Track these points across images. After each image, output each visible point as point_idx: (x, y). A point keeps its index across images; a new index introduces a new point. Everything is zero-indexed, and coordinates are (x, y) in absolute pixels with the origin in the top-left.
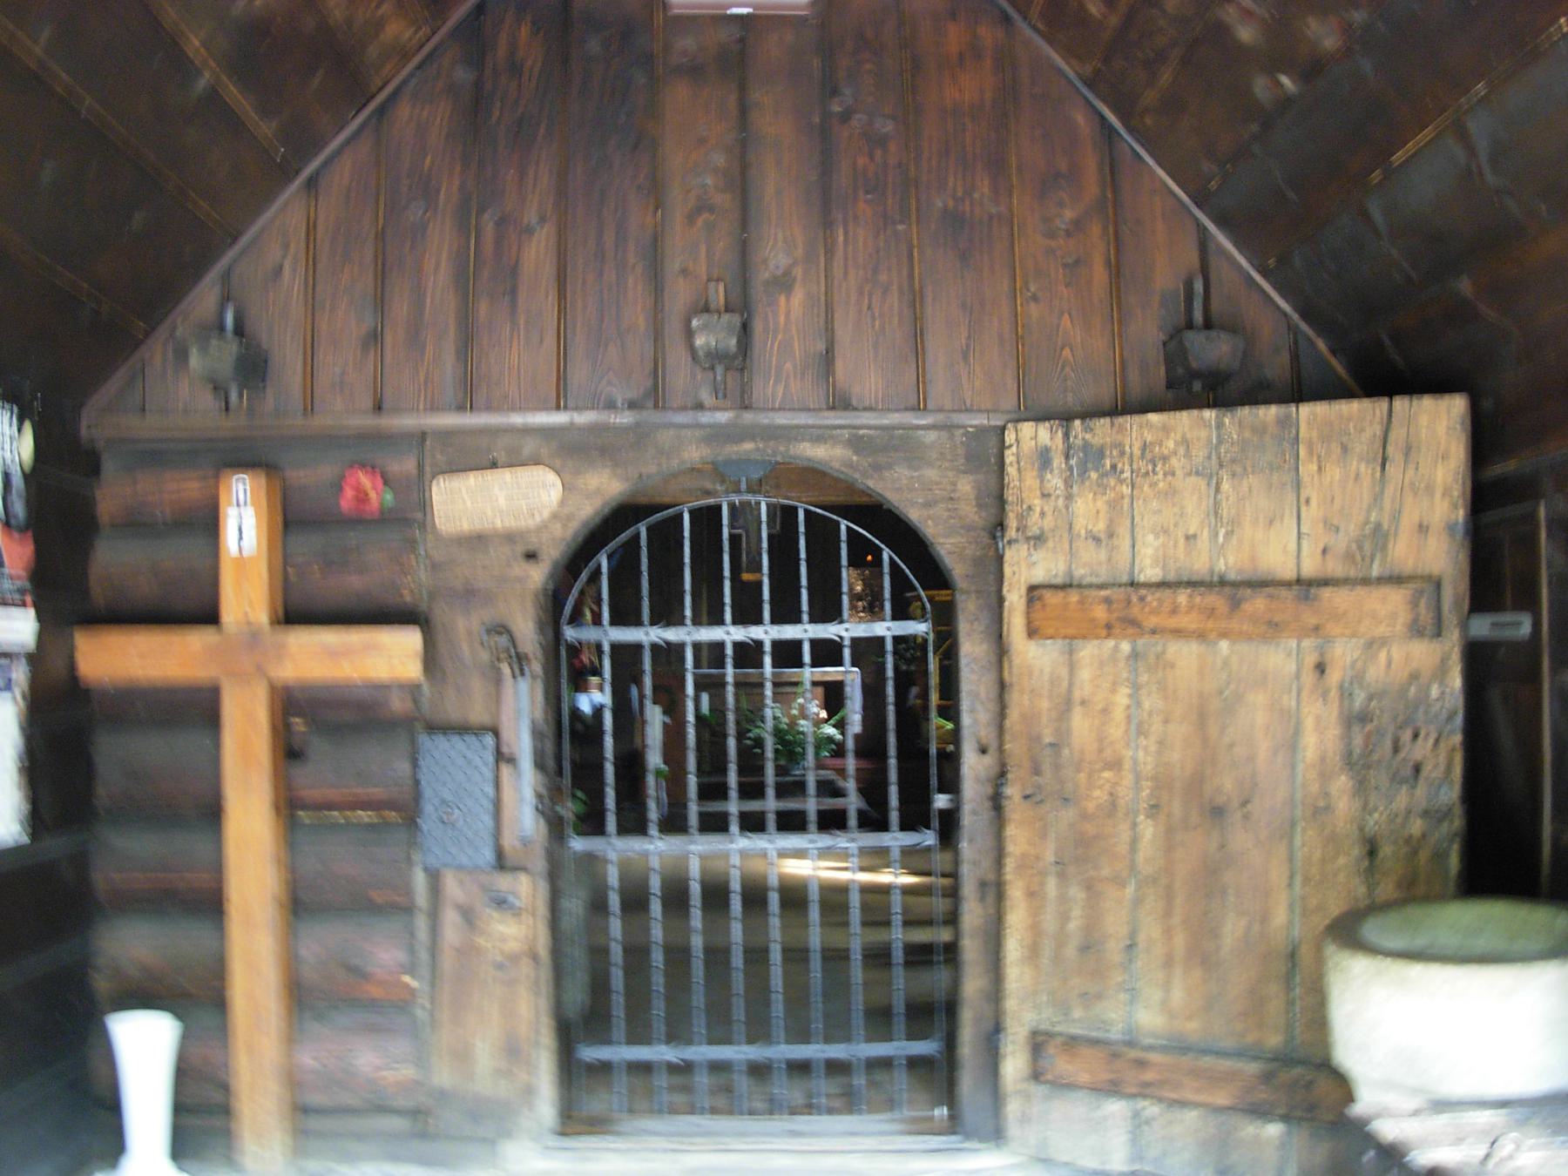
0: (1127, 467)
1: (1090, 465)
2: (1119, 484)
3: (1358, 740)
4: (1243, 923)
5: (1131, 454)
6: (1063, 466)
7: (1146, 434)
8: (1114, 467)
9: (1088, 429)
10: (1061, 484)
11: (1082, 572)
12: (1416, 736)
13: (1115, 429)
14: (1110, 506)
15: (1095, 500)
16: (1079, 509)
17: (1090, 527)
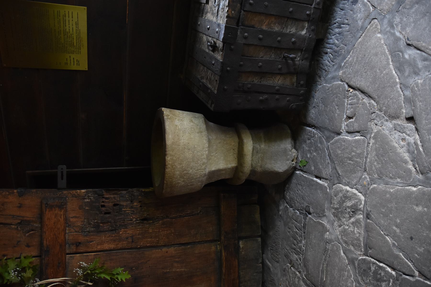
3: (106, 227)
4: (175, 265)
12: (103, 206)
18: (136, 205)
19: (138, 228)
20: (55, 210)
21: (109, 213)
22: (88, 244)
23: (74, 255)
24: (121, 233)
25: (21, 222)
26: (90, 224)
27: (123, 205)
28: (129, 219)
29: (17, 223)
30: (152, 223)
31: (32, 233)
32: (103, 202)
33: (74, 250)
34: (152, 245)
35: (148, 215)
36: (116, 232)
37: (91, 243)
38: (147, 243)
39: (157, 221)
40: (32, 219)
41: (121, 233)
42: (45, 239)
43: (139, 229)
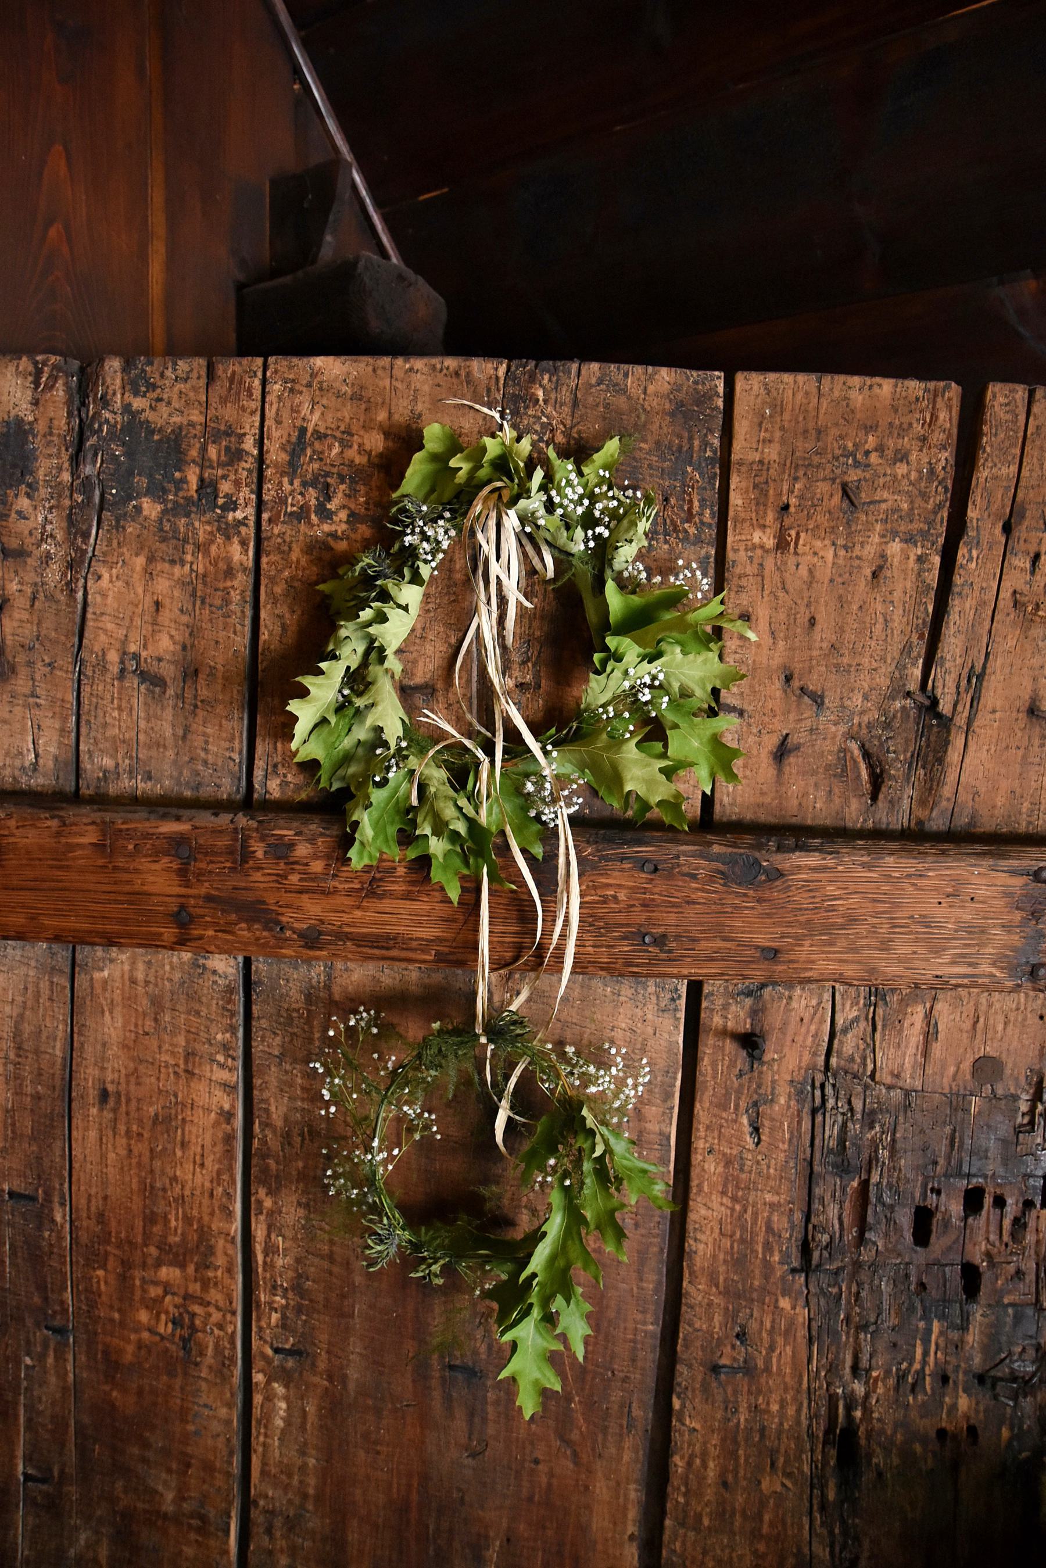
0: (246, 494)
1: (141, 482)
2: (220, 540)
5: (261, 459)
6: (66, 477)
7: (305, 409)
8: (208, 487)
9: (135, 385)
10: (57, 527)
11: (108, 762)
12: (973, 1200)
13: (219, 388)
14: (194, 594)
15: (149, 574)
16: (104, 596)
17: (133, 648)
18: (954, 1407)
19: (799, 1411)
20: (1007, 927)
21: (922, 1234)
22: (743, 1104)
23: (682, 1015)
24: (785, 1303)
25: (939, 716)
26: (870, 1119)
27: (964, 1328)
28: (865, 1359)
29: (939, 692)
30: (823, 1496)
31: (859, 776)
32: (1000, 1202)
33: (717, 1021)
34: (675, 1481)
35: (880, 1475)
36: (794, 1271)
37: (745, 1120)
38: (692, 1457)
39: (831, 1533)
40: (951, 777)
41: (785, 1303)
42: (830, 861)
43: (791, 1411)
